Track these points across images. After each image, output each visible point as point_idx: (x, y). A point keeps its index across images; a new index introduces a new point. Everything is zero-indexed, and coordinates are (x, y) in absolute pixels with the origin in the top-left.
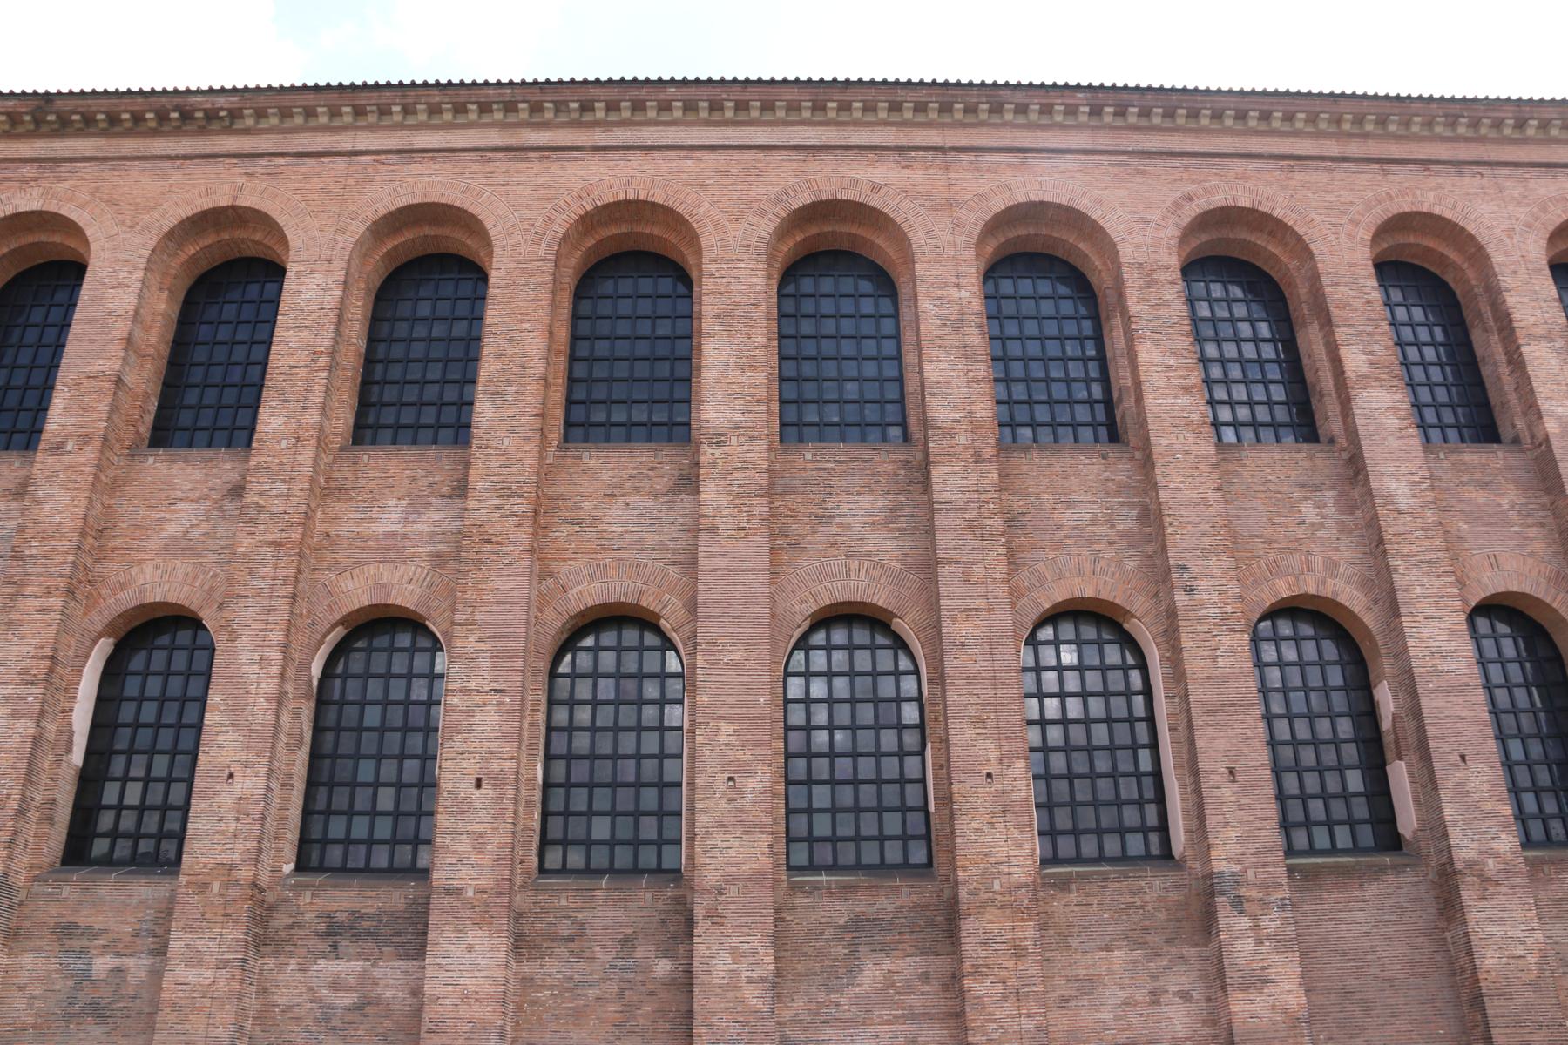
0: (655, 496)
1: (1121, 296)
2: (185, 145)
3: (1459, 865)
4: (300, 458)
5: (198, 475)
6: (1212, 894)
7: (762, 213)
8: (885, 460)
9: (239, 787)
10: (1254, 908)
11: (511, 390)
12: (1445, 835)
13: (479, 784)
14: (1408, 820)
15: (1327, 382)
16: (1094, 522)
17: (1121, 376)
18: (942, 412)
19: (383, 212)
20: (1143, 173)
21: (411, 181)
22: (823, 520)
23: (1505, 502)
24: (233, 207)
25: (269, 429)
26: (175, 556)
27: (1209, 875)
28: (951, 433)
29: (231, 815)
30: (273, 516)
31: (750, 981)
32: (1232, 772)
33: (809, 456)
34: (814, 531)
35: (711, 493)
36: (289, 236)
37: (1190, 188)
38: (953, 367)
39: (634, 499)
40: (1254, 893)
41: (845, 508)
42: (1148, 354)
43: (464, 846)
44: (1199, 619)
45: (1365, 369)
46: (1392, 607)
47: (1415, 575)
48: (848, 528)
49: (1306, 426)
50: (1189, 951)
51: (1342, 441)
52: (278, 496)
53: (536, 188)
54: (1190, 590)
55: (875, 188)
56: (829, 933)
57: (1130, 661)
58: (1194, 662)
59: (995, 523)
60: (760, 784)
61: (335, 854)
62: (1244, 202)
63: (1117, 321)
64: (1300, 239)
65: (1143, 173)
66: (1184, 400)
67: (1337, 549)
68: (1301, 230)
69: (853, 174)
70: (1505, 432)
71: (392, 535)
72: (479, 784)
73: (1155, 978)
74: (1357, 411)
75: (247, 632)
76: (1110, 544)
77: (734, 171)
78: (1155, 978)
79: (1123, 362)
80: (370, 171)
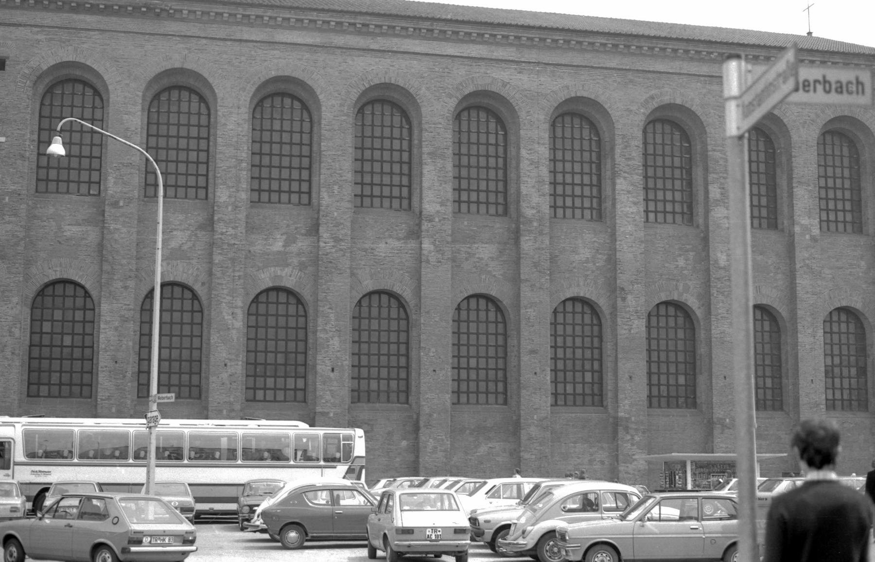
0: (399, 239)
1: (613, 149)
2: (149, 26)
3: (715, 420)
4: (239, 216)
5: (181, 217)
6: (617, 425)
7: (450, 96)
8: (499, 226)
9: (230, 370)
10: (632, 432)
11: (336, 187)
12: (712, 408)
13: (333, 370)
14: (701, 397)
15: (701, 197)
16: (587, 261)
17: (607, 191)
18: (529, 212)
19: (263, 80)
20: (631, 81)
21: (276, 61)
22: (470, 255)
23: (770, 262)
24: (182, 69)
25: (222, 200)
26: (177, 259)
27: (616, 418)
28: (530, 221)
29: (228, 382)
30: (229, 245)
31: (441, 451)
32: (631, 377)
33: (466, 223)
34: (467, 259)
35: (427, 245)
36: (217, 91)
37: (654, 92)
38: (534, 187)
39: (390, 241)
40: (633, 426)
41: (481, 250)
42: (621, 184)
43: (328, 396)
44: (626, 312)
45: (718, 196)
46: (709, 312)
47: (721, 297)
48: (482, 259)
49: (689, 215)
50: (605, 445)
51: (702, 227)
52: (231, 235)
53: (340, 72)
54: (624, 299)
55: (505, 84)
56: (468, 432)
57: (595, 322)
58: (622, 332)
59: (547, 265)
60: (447, 373)
61: (260, 394)
62: (678, 101)
63: (609, 161)
64: (702, 123)
65: (631, 81)
66: (634, 209)
67: (690, 280)
68: (703, 118)
69: (494, 75)
70: (780, 227)
71: (279, 253)
72: (333, 370)
73: (591, 455)
74: (710, 218)
75: (224, 301)
76: (593, 272)
77: (437, 69)
78: (591, 455)
79: (609, 182)
80: (253, 53)
